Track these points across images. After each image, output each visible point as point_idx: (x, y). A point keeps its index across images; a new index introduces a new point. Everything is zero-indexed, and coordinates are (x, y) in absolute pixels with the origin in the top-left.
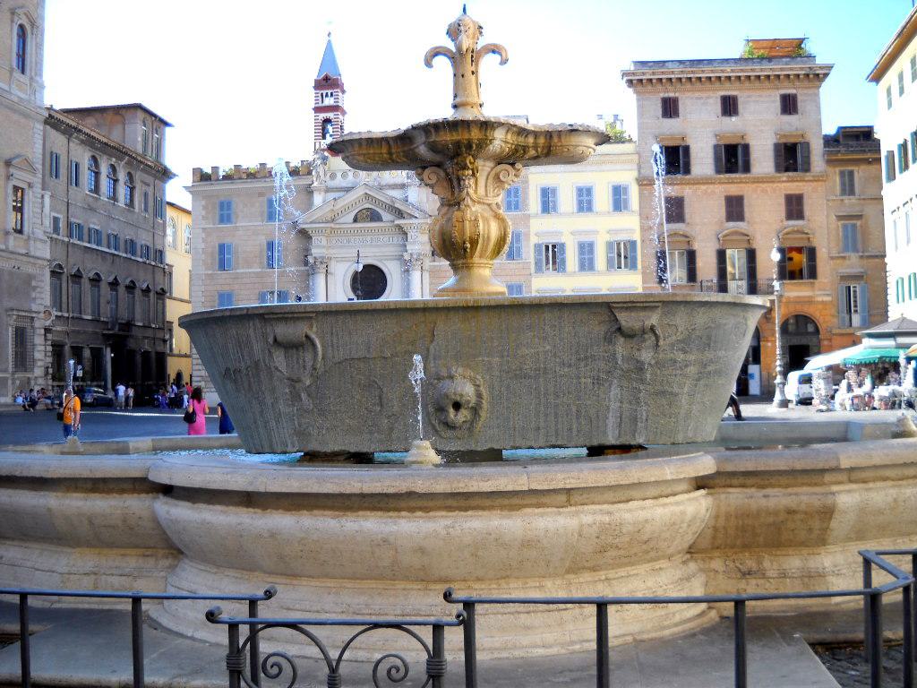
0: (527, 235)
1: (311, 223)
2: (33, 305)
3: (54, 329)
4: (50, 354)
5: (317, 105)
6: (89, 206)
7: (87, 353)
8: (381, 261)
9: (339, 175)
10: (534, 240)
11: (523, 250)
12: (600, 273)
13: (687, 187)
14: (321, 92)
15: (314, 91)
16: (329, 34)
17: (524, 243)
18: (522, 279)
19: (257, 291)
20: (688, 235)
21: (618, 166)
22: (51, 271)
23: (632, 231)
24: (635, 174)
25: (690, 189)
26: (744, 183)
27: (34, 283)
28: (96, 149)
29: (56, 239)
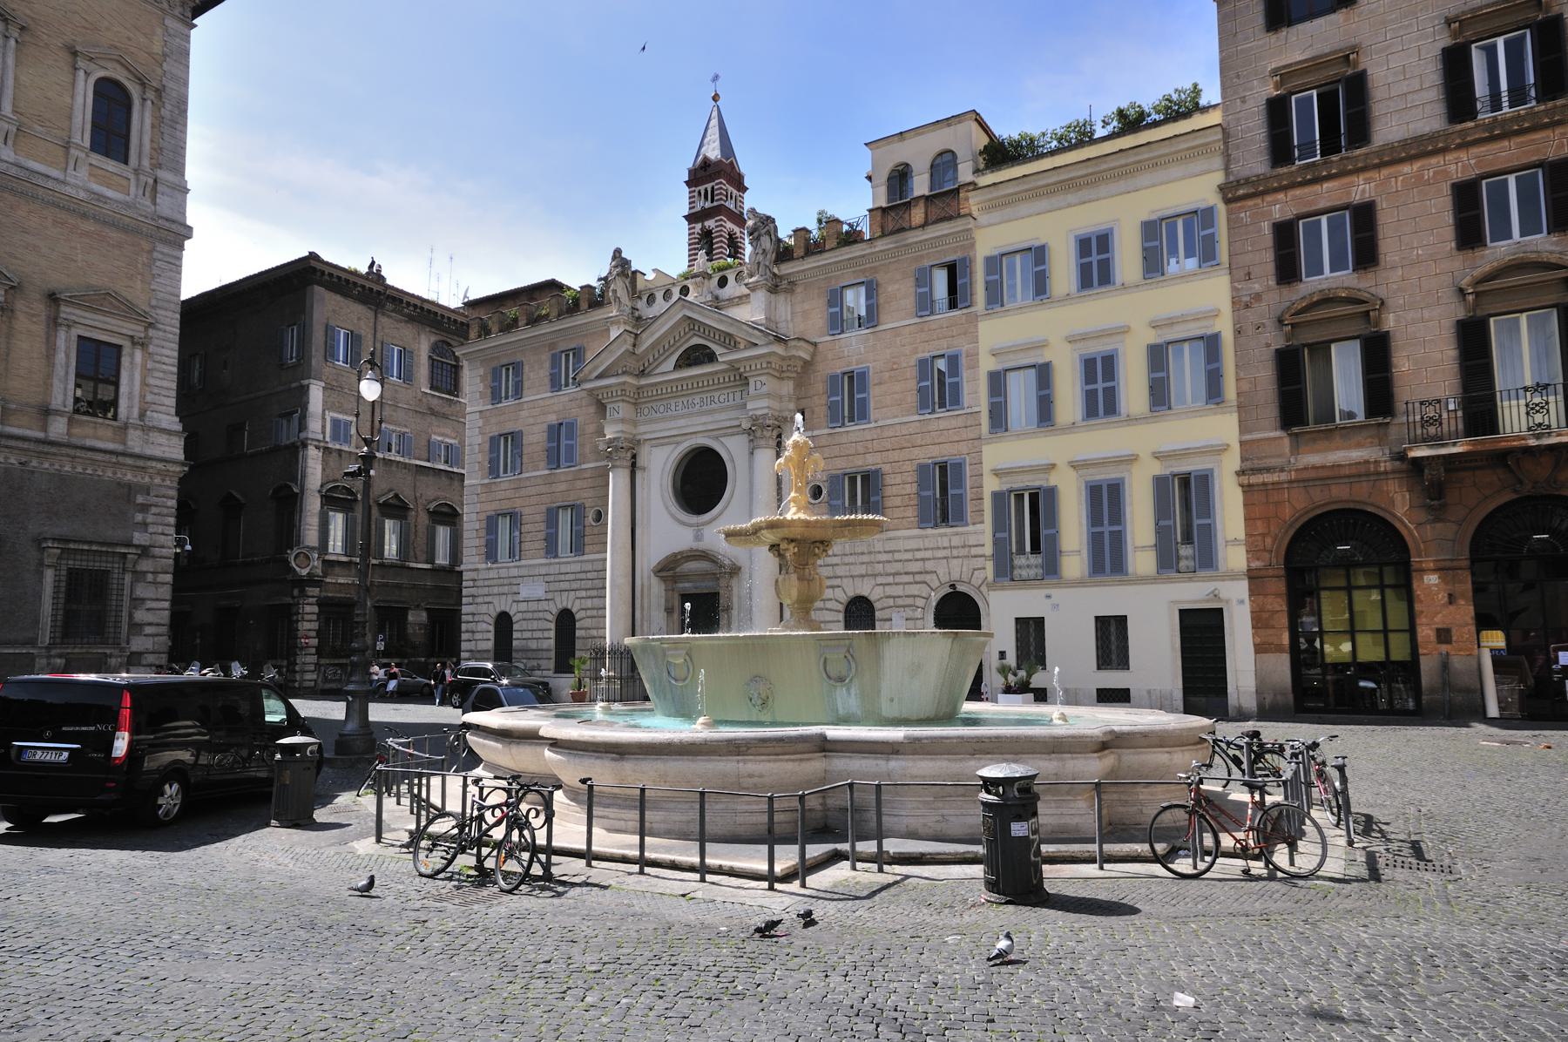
0: (973, 356)
1: (598, 377)
2: (136, 535)
3: (328, 580)
4: (315, 617)
5: (693, 211)
6: (430, 409)
7: (417, 617)
8: (717, 438)
9: (659, 295)
10: (987, 364)
11: (966, 389)
12: (1132, 420)
13: (1362, 178)
14: (697, 189)
15: (687, 189)
16: (716, 98)
17: (965, 374)
18: (963, 448)
19: (544, 508)
20: (1365, 296)
21: (1175, 171)
22: (322, 496)
23: (1216, 314)
24: (1219, 178)
25: (1367, 181)
26: (1545, 127)
27: (140, 499)
28: (448, 331)
29: (340, 451)
